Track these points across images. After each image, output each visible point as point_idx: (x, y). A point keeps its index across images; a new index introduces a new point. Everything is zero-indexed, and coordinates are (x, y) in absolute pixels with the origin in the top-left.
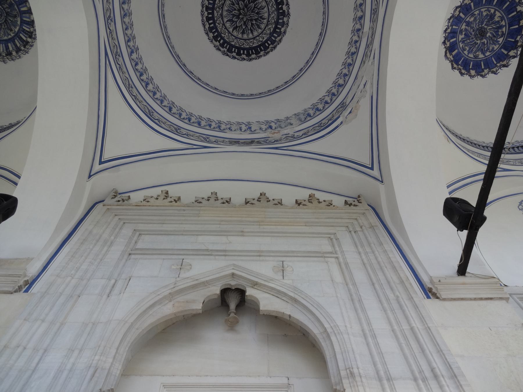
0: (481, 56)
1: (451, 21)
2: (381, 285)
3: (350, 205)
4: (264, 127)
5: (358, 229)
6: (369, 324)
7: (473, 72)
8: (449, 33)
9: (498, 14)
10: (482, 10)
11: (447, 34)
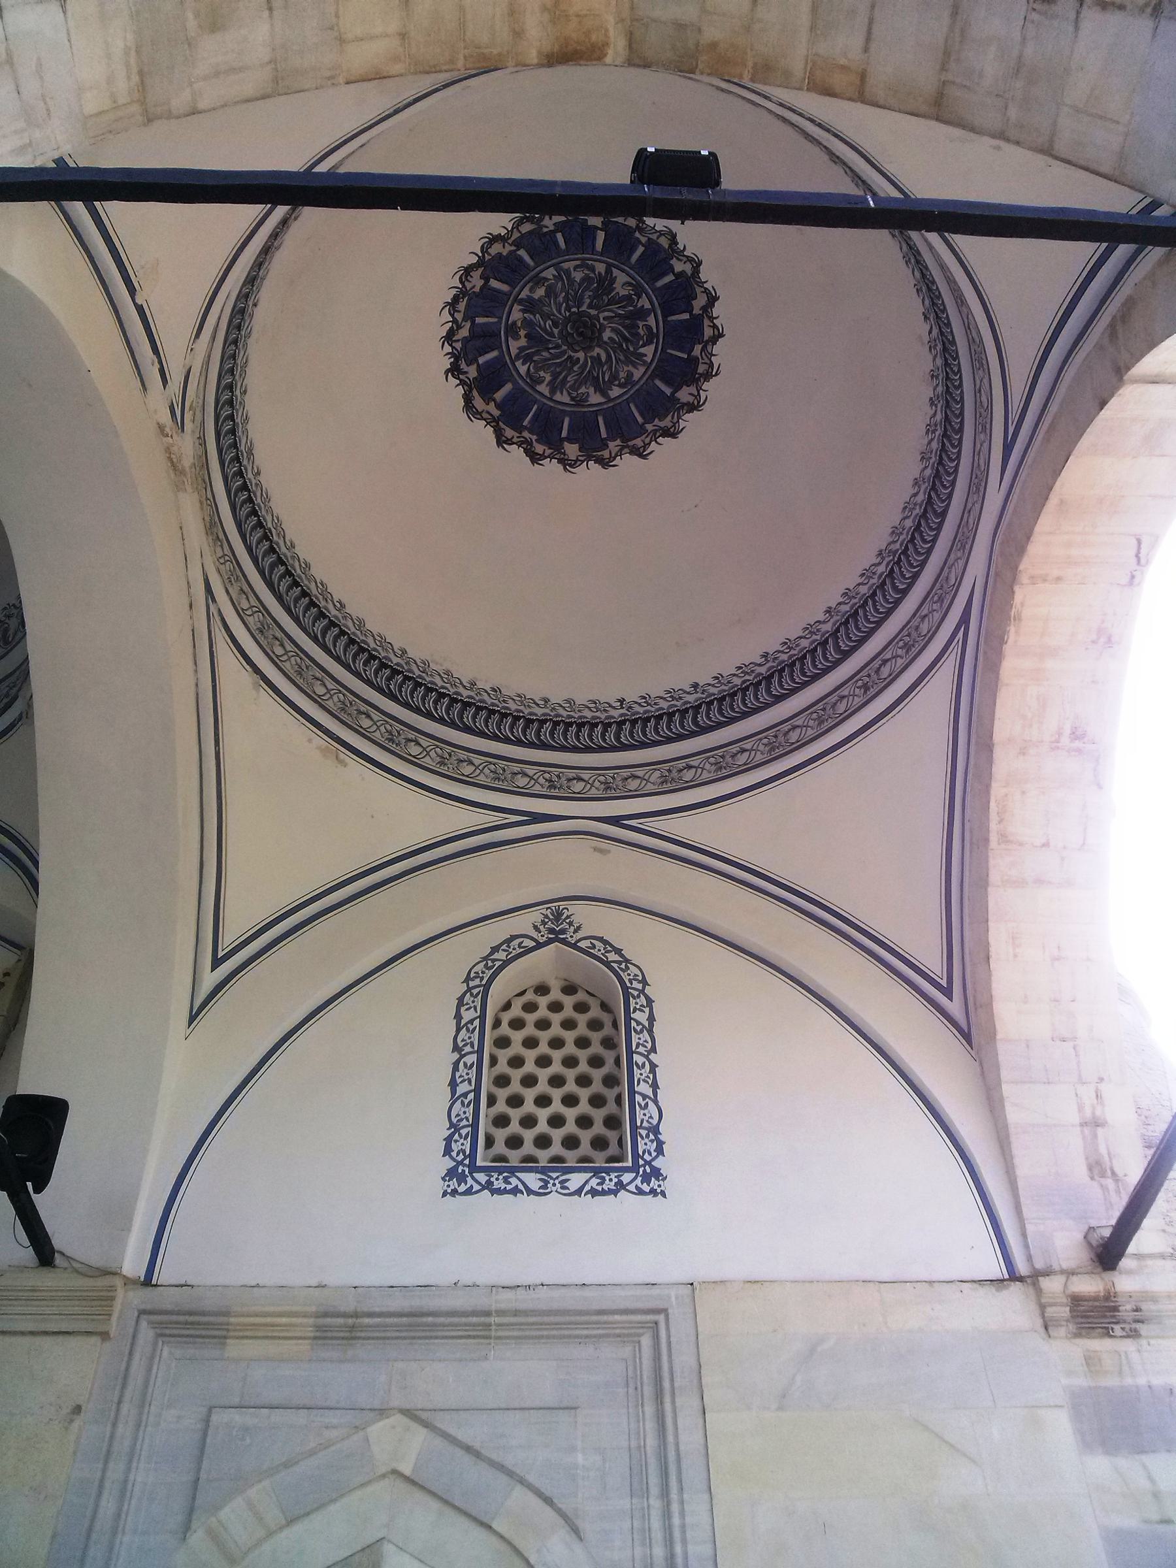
0: (595, 398)
1: (462, 306)
7: (572, 450)
8: (465, 341)
9: (621, 278)
10: (565, 265)
11: (458, 345)
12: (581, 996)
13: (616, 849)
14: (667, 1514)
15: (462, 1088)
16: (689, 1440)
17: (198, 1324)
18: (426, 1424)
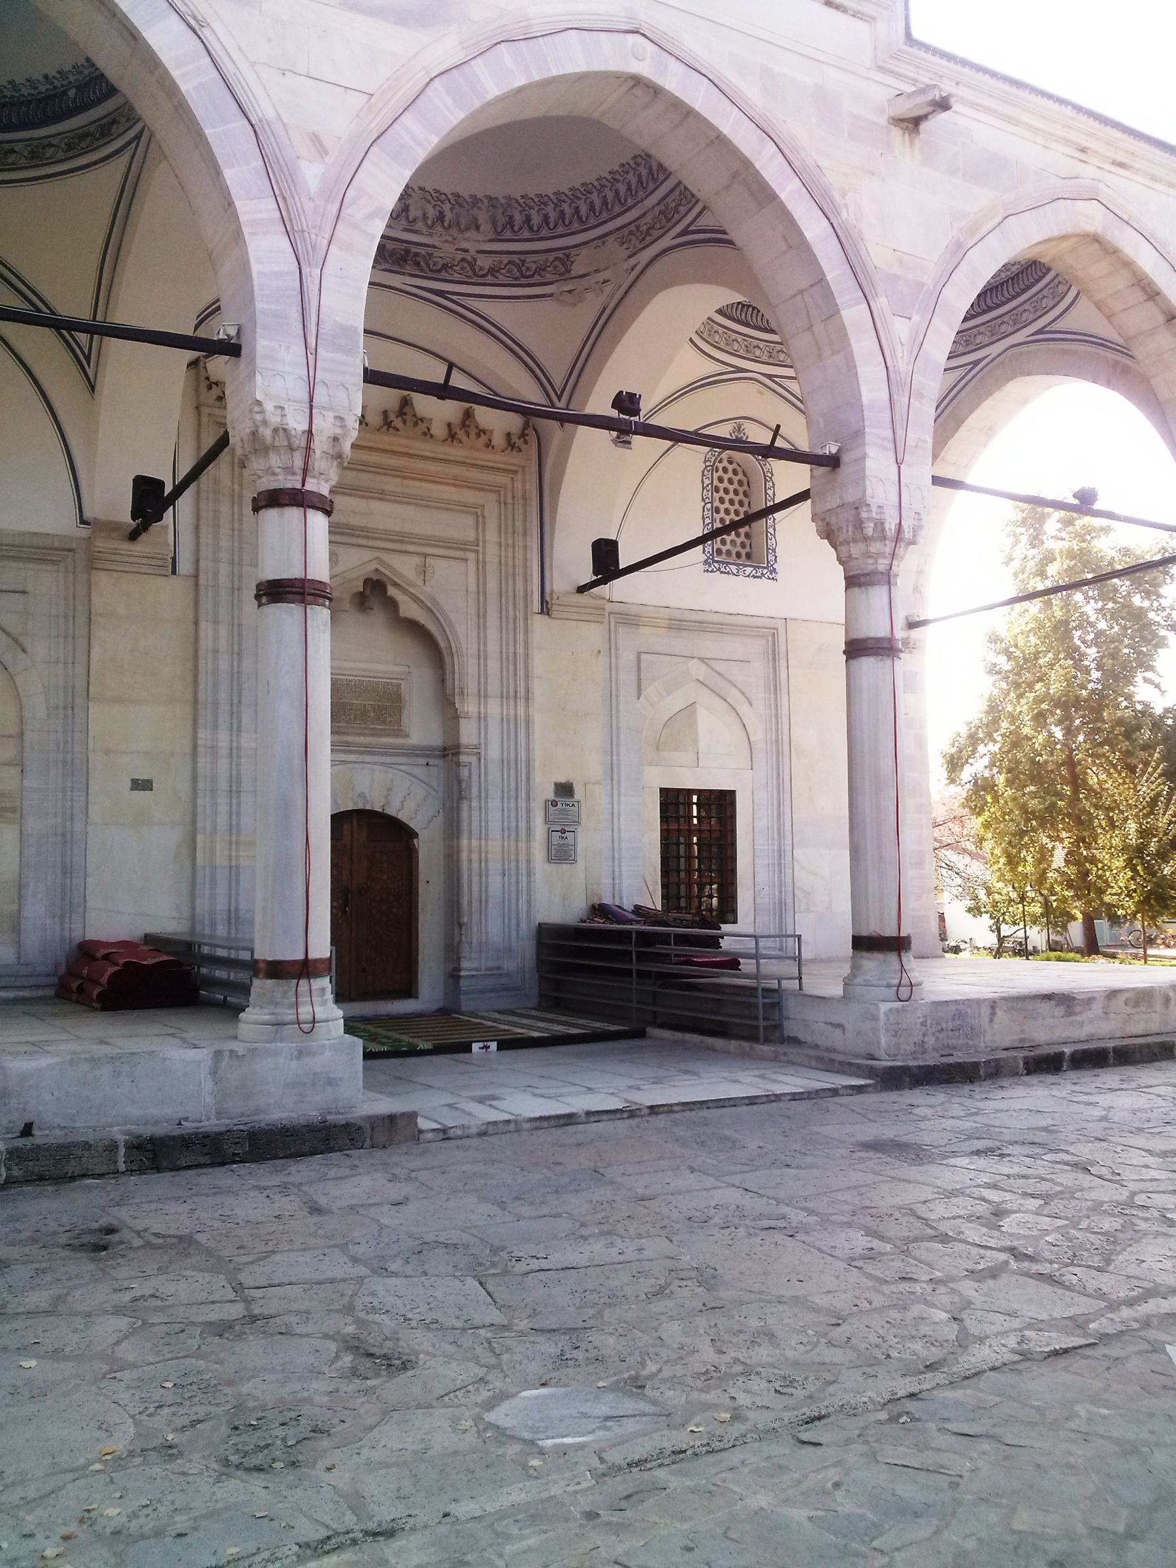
2: (507, 597)
3: (511, 446)
4: (432, 213)
5: (510, 500)
6: (485, 644)
12: (735, 466)
13: (769, 394)
14: (776, 701)
15: (707, 521)
16: (783, 676)
17: (629, 619)
18: (707, 665)
